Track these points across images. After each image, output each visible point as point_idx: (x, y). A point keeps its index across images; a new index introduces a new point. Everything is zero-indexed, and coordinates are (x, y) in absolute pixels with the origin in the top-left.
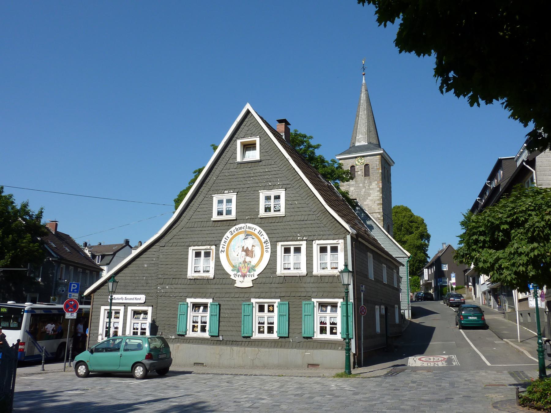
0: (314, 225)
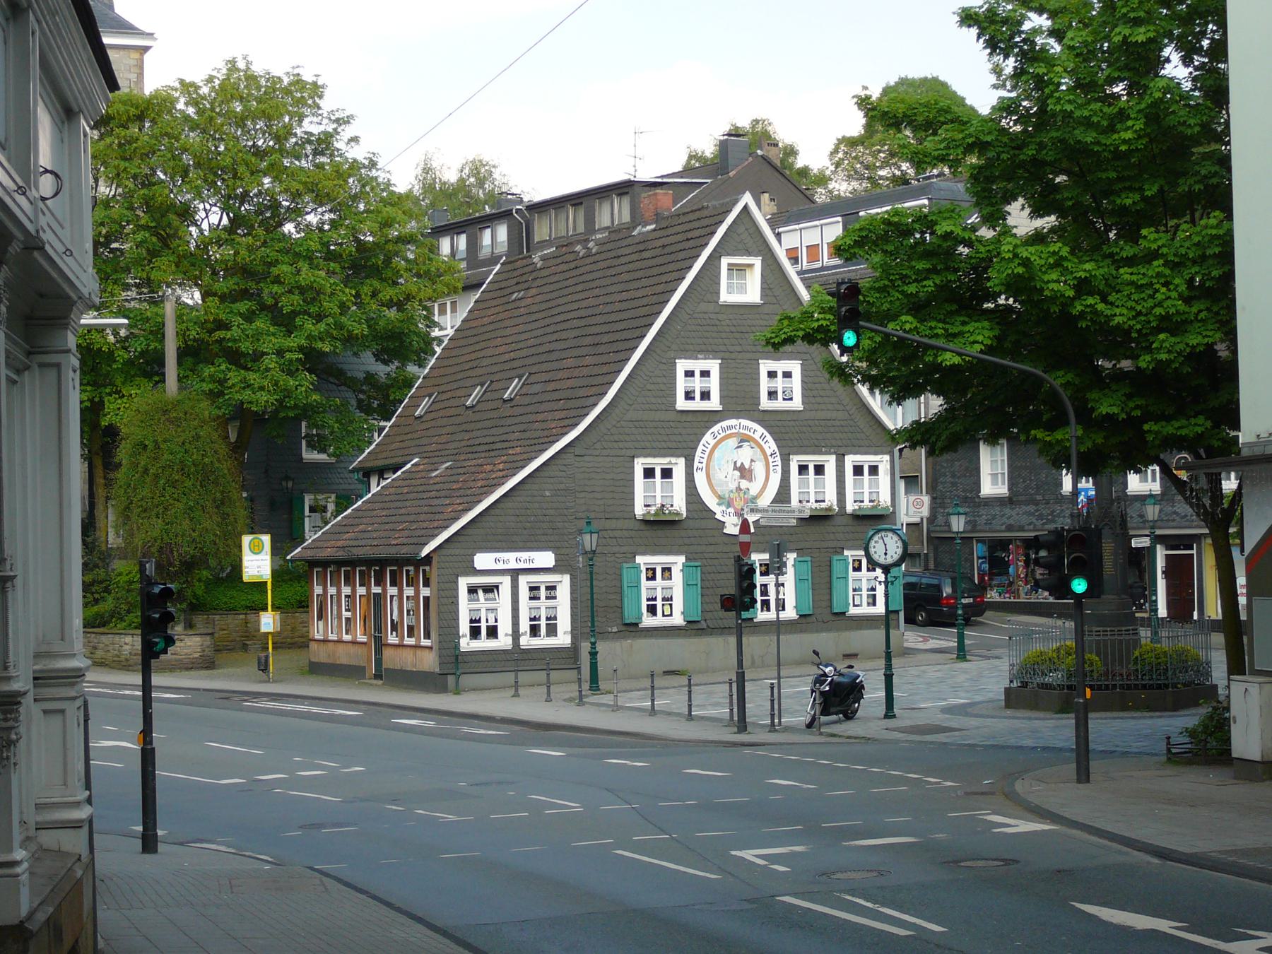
0: (846, 429)
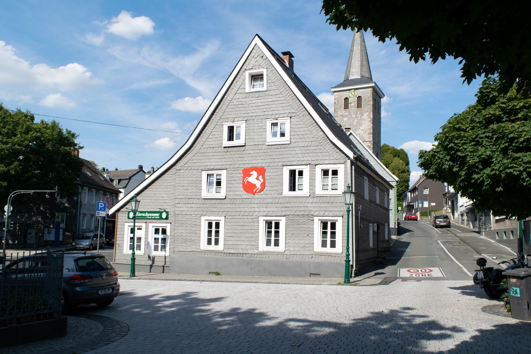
0: (317, 151)
